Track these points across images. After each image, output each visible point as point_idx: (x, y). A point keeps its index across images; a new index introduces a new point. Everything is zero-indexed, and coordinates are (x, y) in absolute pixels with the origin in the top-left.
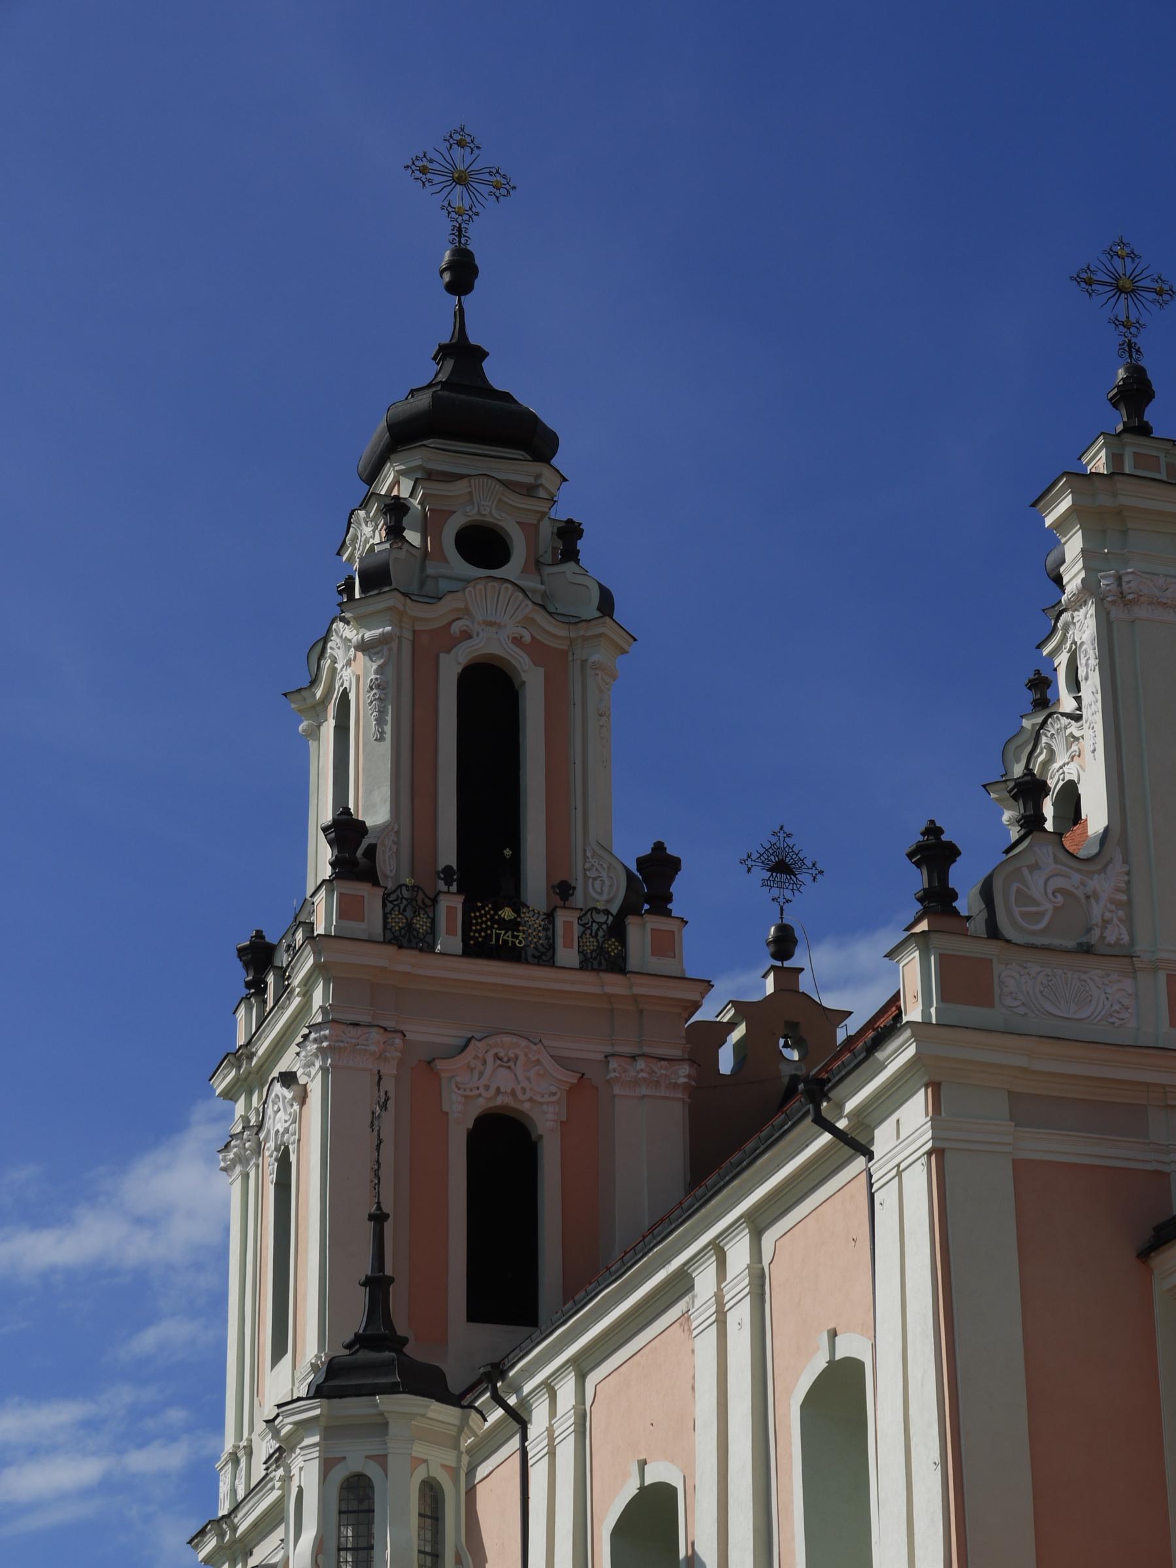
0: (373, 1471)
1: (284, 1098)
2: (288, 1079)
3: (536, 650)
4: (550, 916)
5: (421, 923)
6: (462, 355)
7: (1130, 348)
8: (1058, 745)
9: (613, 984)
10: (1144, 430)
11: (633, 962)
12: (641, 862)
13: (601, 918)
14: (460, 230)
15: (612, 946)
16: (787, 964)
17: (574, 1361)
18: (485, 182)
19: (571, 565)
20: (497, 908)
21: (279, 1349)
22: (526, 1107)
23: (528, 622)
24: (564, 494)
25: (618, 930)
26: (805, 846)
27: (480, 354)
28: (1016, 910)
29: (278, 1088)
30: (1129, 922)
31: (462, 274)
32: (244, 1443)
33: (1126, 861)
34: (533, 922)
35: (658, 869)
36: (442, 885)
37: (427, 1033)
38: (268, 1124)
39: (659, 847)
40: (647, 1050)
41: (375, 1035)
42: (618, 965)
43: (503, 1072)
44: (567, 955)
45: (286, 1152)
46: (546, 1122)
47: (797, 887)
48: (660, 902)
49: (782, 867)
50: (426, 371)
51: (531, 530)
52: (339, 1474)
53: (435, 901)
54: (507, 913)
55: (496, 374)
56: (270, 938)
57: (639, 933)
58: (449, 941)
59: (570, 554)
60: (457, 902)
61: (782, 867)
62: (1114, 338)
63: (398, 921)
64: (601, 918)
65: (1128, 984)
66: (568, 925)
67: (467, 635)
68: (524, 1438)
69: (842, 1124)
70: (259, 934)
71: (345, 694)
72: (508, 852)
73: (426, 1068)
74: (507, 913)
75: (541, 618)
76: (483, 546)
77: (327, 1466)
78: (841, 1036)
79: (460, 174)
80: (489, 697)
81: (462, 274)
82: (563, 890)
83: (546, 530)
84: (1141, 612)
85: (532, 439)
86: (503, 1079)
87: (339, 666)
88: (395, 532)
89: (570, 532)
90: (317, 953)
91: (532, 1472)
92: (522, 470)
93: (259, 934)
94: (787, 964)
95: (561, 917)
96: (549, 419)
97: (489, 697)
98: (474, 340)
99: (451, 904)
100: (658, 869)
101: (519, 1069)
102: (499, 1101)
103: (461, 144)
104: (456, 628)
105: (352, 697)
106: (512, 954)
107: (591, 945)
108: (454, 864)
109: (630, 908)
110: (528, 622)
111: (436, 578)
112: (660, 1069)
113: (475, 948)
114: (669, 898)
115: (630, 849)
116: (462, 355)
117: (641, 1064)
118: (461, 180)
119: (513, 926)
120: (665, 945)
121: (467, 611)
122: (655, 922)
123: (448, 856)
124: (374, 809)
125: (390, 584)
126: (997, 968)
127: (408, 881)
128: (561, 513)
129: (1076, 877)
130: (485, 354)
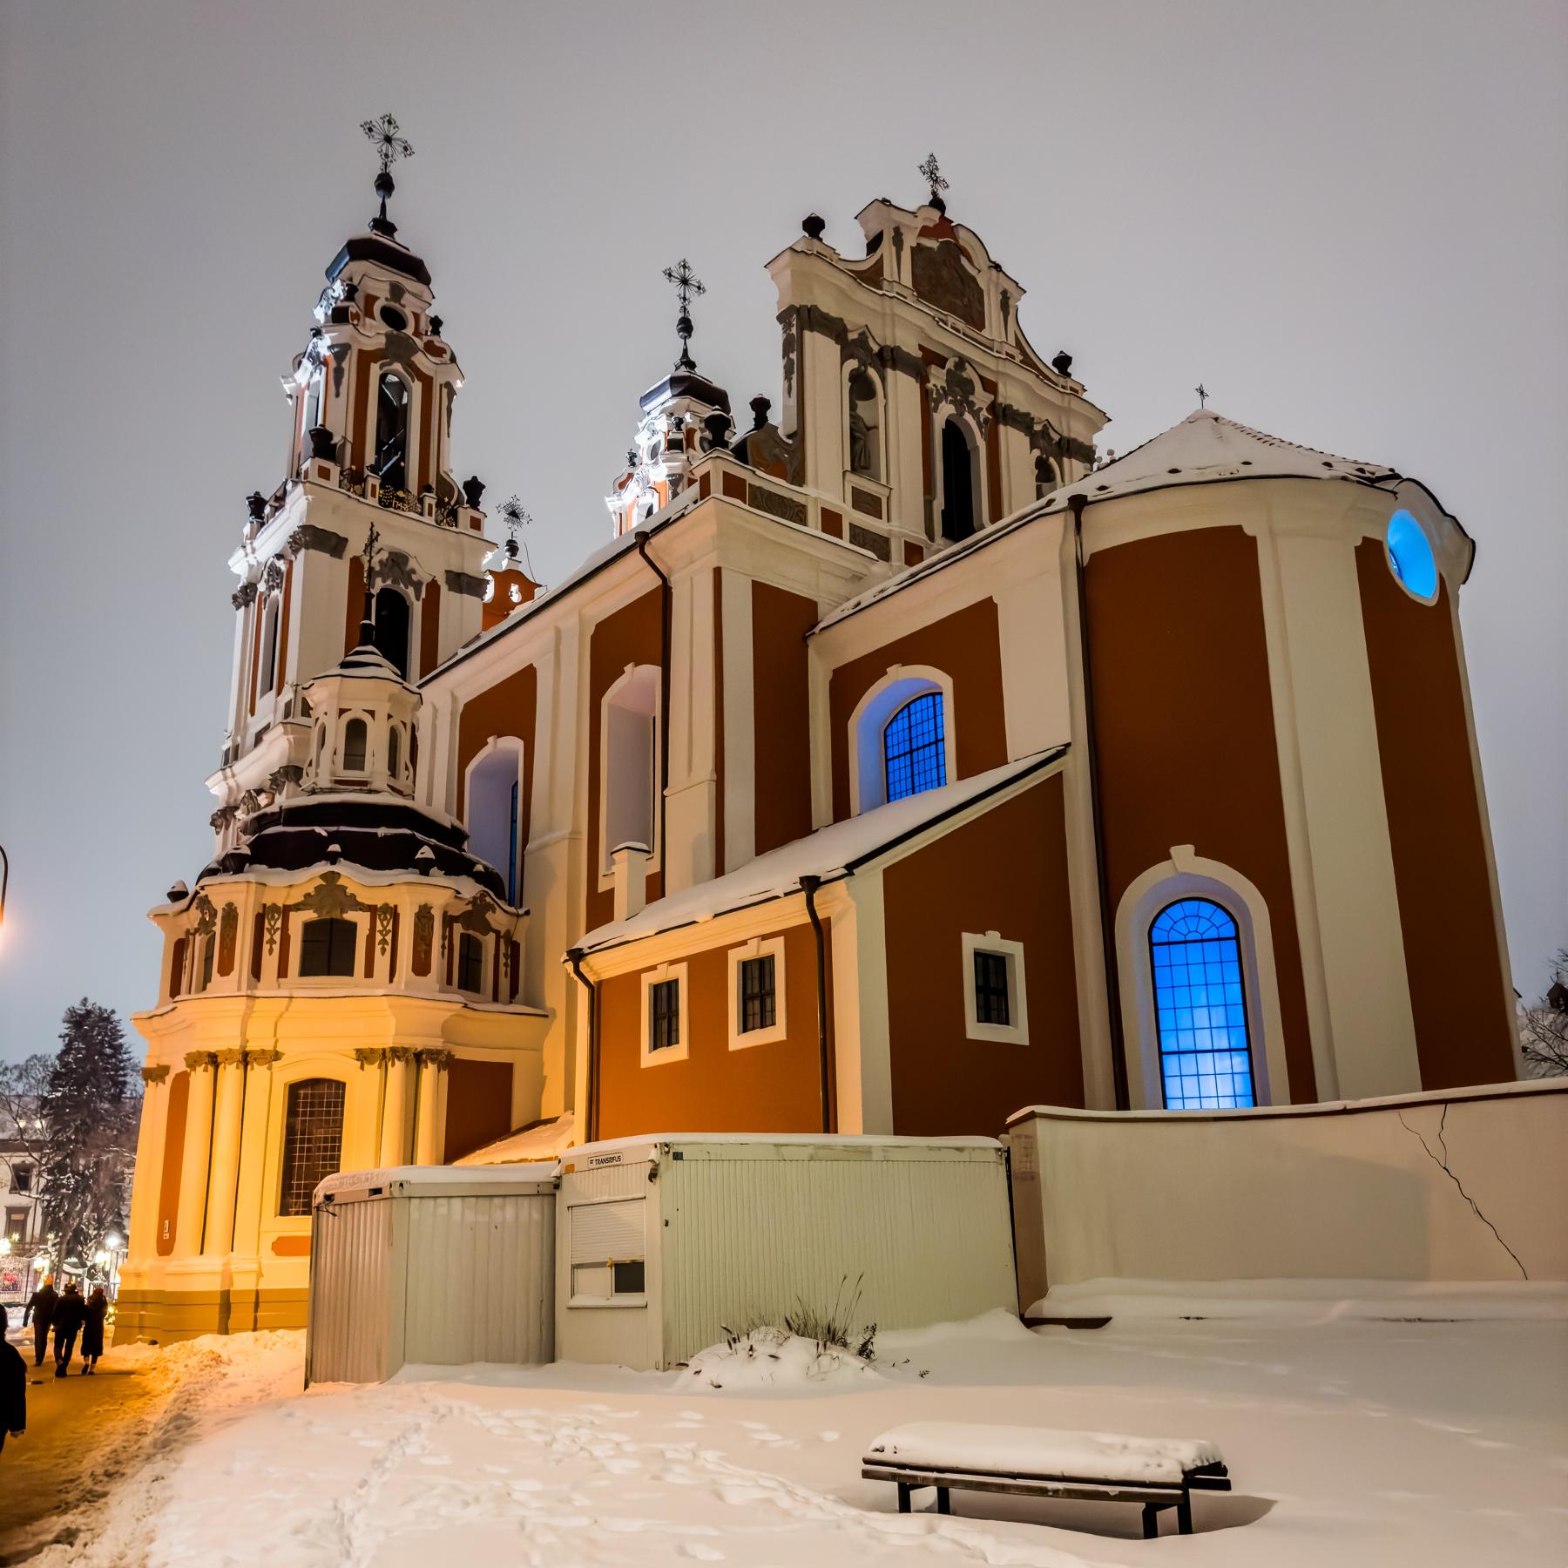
6: (383, 225)
12: (467, 485)
26: (524, 506)
35: (474, 488)
47: (520, 524)
48: (474, 503)
49: (514, 514)
51: (417, 316)
54: (401, 494)
59: (436, 332)
60: (377, 482)
61: (514, 514)
74: (401, 494)
89: (436, 323)
98: (389, 218)
103: (390, 122)
116: (383, 225)
124: (341, 431)
128: (431, 312)
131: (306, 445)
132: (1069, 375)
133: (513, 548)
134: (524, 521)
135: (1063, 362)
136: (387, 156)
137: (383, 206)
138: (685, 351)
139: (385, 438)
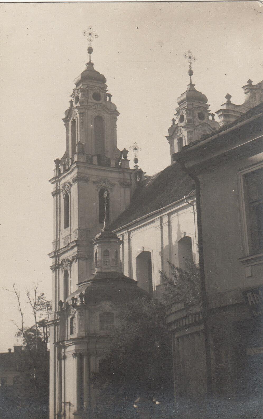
1: (67, 185)
7: (190, 67)
14: (90, 43)
18: (94, 35)
21: (67, 225)
31: (90, 51)
32: (58, 239)
35: (125, 152)
43: (104, 184)
55: (96, 68)
62: (188, 65)
81: (90, 51)
90: (77, 164)
114: (127, 157)
116: (90, 65)
118: (90, 34)
134: (139, 150)
136: (90, 40)
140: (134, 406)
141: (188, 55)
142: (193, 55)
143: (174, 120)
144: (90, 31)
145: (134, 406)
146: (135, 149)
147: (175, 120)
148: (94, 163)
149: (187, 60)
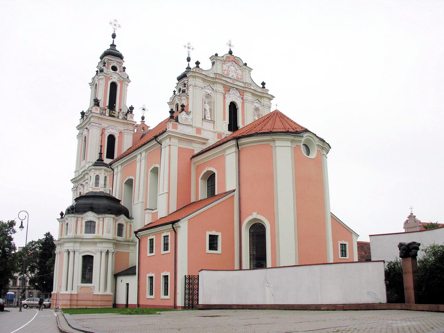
0: (99, 175)
2: (87, 128)
3: (119, 81)
4: (119, 113)
5: (104, 112)
6: (113, 46)
8: (177, 99)
9: (125, 121)
10: (199, 67)
11: (128, 119)
12: (130, 108)
13: (125, 113)
15: (126, 117)
16: (143, 120)
17: (121, 164)
19: (124, 72)
20: (113, 111)
22: (114, 134)
23: (119, 78)
24: (124, 63)
25: (126, 115)
26: (146, 108)
27: (115, 46)
28: (180, 119)
29: (85, 129)
30: (192, 122)
31: (114, 36)
33: (193, 115)
34: (117, 113)
35: (132, 108)
36: (107, 108)
37: (104, 125)
38: (83, 133)
39: (132, 106)
40: (129, 129)
41: (98, 124)
42: (126, 119)
44: (120, 117)
45: (86, 136)
46: (117, 136)
48: (131, 112)
50: (109, 47)
52: (96, 175)
53: (106, 109)
54: (114, 112)
55: (117, 48)
56: (85, 112)
57: (129, 116)
58: (107, 115)
59: (124, 71)
60: (109, 110)
61: (144, 109)
62: (188, 53)
63: (101, 111)
64: (125, 113)
65: (192, 129)
66: (121, 114)
67: (112, 79)
68: (114, 172)
69: (158, 141)
70: (83, 111)
71: (96, 85)
72: (115, 105)
73: (103, 130)
74: (114, 112)
75: (120, 78)
76: (114, 69)
77: (94, 173)
78: (149, 129)
79: (115, 24)
80: (114, 86)
81: (114, 36)
82: (121, 110)
83: (122, 67)
84: (197, 88)
85: (120, 57)
86: (112, 131)
87: (96, 81)
88: (104, 66)
89: (124, 68)
91: (114, 176)
92: (120, 60)
93: (83, 111)
94: (143, 120)
95: (120, 113)
96: (123, 55)
97: (114, 86)
99: (108, 110)
100: (132, 108)
101: (114, 130)
102: (111, 133)
104: (110, 78)
105: (97, 85)
106: (114, 116)
107: (123, 116)
108: (108, 105)
109: (128, 112)
110: (119, 78)
111: (109, 72)
112: (130, 131)
113: (110, 116)
115: (128, 106)
116: (113, 46)
117: (128, 131)
119: (114, 113)
120: (132, 117)
121: (112, 76)
122: (131, 114)
123: (107, 104)
125: (103, 72)
126: (178, 126)
127: (103, 107)
128: (123, 66)
129: (187, 116)
130: (116, 46)
131: (93, 103)
132: (265, 87)
133: (143, 118)
135: (263, 84)
137: (113, 40)
138: (189, 65)
139: (111, 100)
140: (44, 283)
141: (187, 45)
142: (191, 46)
143: (174, 92)
144: (115, 23)
145: (44, 283)
146: (144, 109)
147: (176, 91)
148: (106, 115)
149: (186, 50)
